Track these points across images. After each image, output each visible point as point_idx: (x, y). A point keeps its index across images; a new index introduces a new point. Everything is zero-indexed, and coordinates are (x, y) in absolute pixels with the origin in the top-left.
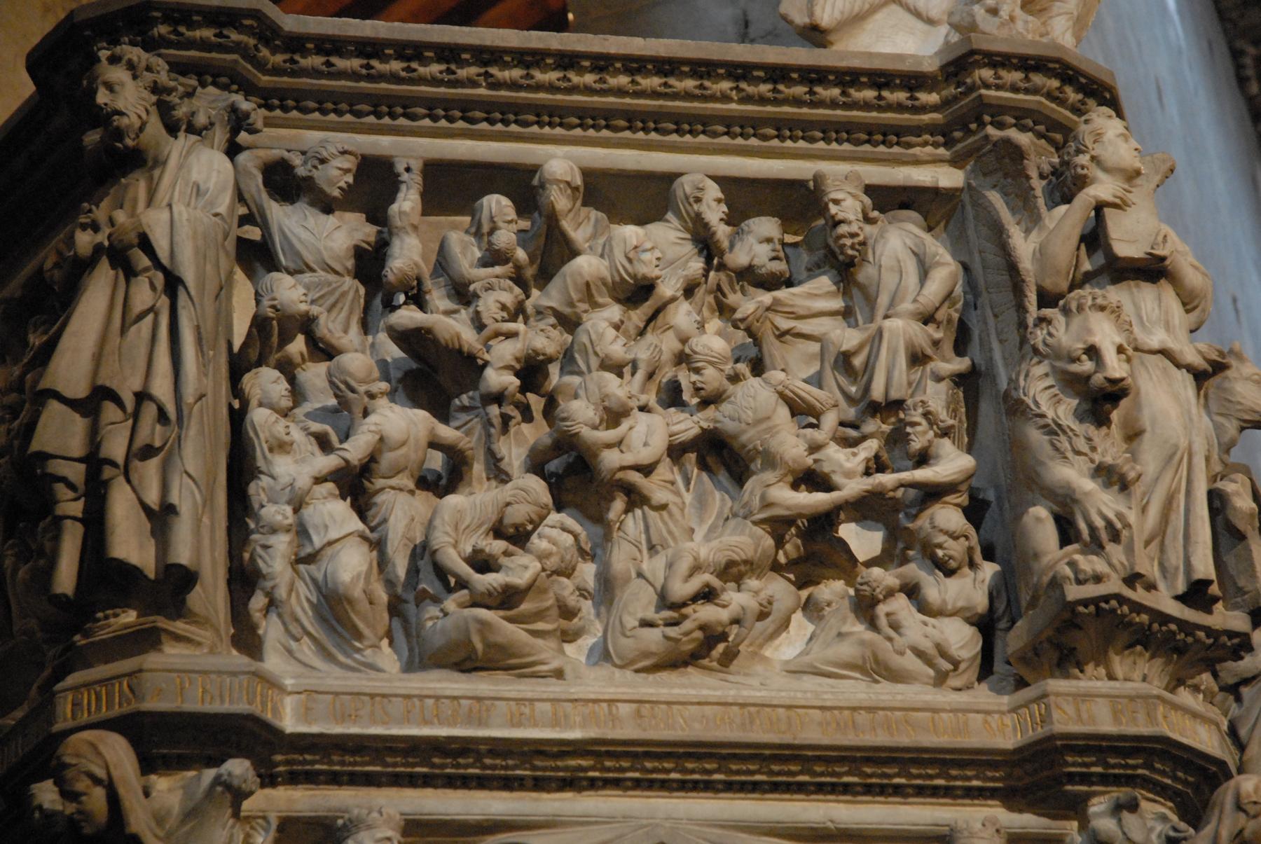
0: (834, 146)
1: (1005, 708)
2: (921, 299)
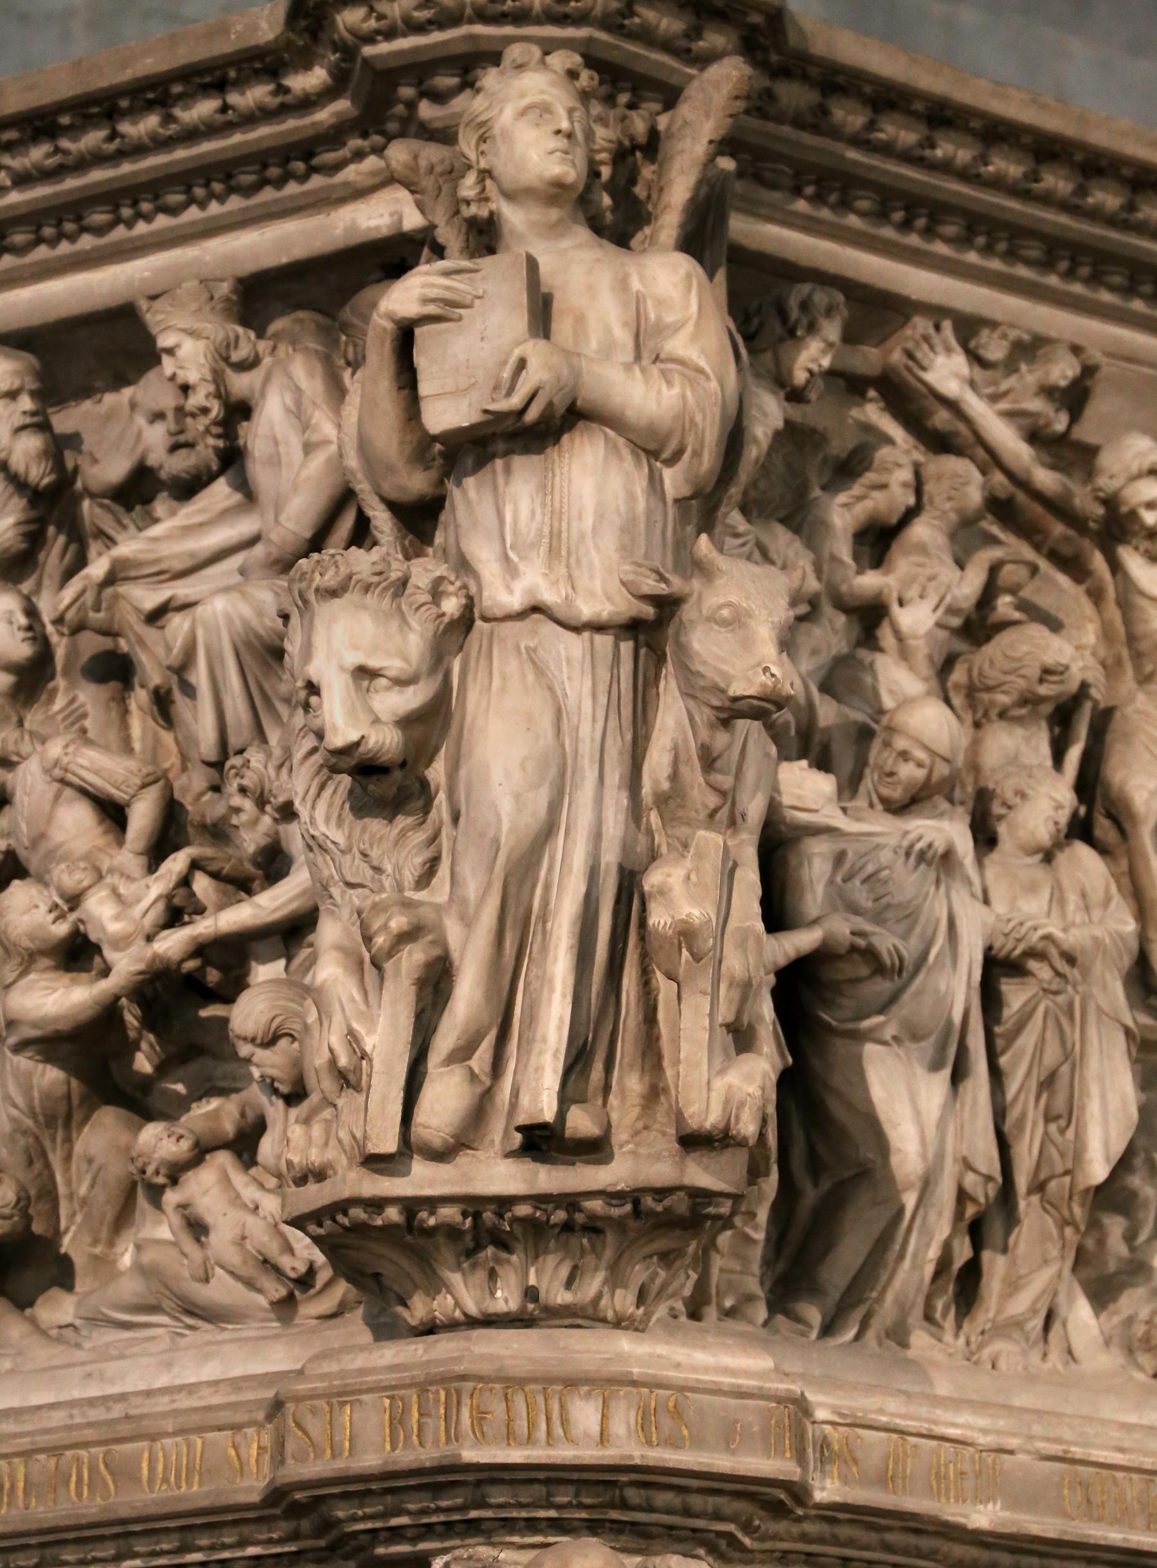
0: (214, 208)
1: (260, 1415)
2: (274, 536)
